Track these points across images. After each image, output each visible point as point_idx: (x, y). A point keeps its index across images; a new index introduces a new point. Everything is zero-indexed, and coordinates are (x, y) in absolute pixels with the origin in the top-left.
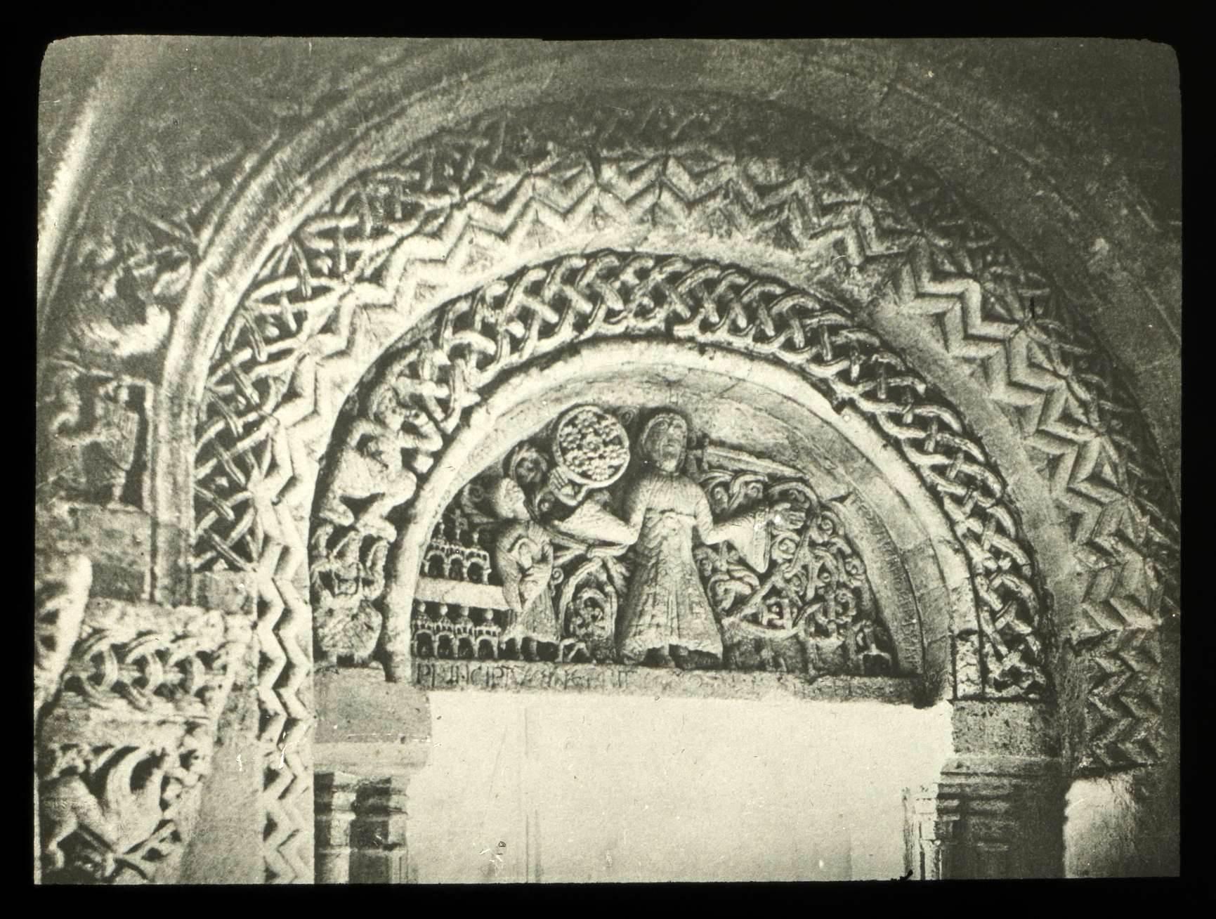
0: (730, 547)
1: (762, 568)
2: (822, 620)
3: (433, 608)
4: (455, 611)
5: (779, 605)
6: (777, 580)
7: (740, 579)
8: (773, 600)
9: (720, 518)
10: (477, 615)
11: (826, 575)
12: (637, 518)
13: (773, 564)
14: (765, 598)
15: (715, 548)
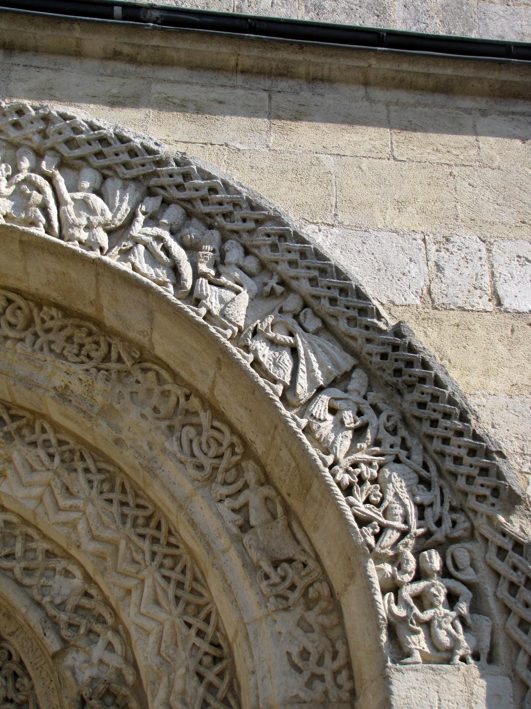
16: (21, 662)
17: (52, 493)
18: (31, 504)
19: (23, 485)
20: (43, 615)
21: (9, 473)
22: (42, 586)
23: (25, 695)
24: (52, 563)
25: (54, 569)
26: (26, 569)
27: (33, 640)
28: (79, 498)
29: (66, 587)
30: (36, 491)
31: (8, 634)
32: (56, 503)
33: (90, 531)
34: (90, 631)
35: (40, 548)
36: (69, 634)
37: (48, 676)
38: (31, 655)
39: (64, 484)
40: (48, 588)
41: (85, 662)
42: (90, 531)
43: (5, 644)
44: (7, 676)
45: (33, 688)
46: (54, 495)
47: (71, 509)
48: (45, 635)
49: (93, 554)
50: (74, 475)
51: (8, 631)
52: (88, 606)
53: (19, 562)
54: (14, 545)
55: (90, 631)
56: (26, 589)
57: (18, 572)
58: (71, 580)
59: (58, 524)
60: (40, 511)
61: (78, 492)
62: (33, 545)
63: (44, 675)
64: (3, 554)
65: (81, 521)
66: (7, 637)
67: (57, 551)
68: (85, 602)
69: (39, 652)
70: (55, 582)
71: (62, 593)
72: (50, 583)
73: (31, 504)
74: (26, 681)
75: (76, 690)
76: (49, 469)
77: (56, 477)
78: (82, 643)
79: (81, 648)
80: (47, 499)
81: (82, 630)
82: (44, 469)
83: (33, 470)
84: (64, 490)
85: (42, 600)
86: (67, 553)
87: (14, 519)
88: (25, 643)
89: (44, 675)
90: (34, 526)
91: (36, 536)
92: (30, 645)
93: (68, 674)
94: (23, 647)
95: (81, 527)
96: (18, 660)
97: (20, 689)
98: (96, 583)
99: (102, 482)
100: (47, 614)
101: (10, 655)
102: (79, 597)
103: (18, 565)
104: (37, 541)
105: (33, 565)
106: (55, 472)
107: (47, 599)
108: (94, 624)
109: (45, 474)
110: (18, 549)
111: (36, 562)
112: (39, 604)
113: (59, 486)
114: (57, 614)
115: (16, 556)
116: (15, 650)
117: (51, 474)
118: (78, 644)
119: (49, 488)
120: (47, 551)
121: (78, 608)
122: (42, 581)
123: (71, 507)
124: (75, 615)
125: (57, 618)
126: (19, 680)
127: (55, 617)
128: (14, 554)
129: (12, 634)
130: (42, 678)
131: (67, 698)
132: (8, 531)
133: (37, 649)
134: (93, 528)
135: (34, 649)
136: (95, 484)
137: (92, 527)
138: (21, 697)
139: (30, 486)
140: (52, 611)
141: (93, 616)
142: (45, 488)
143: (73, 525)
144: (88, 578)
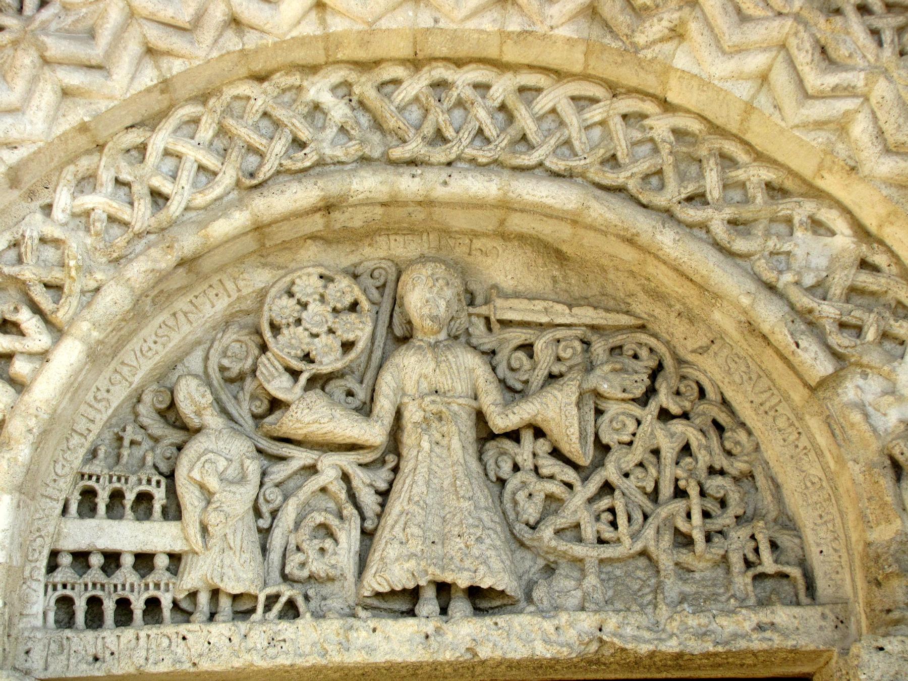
0: (539, 433)
1: (585, 456)
2: (683, 526)
3: (81, 558)
4: (112, 559)
5: (612, 510)
6: (611, 472)
7: (552, 477)
8: (605, 503)
9: (514, 392)
10: (144, 561)
11: (688, 460)
12: (384, 406)
13: (603, 449)
14: (591, 501)
15: (514, 436)
16: (725, 402)
17: (791, 63)
18: (743, 91)
19: (724, 53)
20: (787, 309)
21: (694, 27)
22: (771, 253)
23: (746, 462)
24: (784, 208)
25: (789, 221)
26: (733, 223)
27: (749, 361)
28: (853, 69)
29: (821, 253)
30: (755, 62)
31: (693, 351)
32: (800, 82)
33: (880, 133)
34: (885, 335)
35: (755, 180)
36: (846, 342)
37: (792, 424)
38: (749, 389)
39: (817, 41)
40: (782, 258)
41: (885, 393)
42: (880, 133)
43: (690, 370)
44: (705, 428)
45: (757, 448)
46: (795, 68)
47: (837, 92)
48: (798, 345)
49: (889, 183)
50: (838, 19)
51: (691, 344)
52: (874, 288)
53: (718, 209)
54: (701, 176)
55: (885, 335)
56: (739, 261)
57: (719, 229)
58: (828, 240)
59: (804, 126)
60: (763, 101)
61: (850, 56)
62: (740, 174)
63: (781, 423)
64: (683, 196)
65: (860, 116)
66: (690, 357)
67: (789, 184)
68: (865, 279)
69: (765, 383)
70: (796, 245)
71: (813, 265)
72: (786, 247)
73: (743, 91)
74: (742, 436)
75: (875, 445)
76: (780, 14)
77: (801, 28)
78: (873, 357)
79: (871, 368)
80: (781, 77)
81: (871, 334)
82: (770, 14)
83: (743, 18)
84: (817, 56)
85: (778, 280)
86: (811, 186)
87: (695, 126)
88: (733, 365)
89: (781, 423)
90: (735, 136)
91: (741, 156)
92: (744, 368)
93: (856, 417)
94: (729, 372)
95: (861, 129)
96: (719, 398)
97: (734, 451)
98: (881, 242)
99: (900, 30)
100: (792, 306)
101: (702, 393)
102: (853, 271)
103: (717, 215)
104: (746, 165)
105: (746, 213)
106: (797, 17)
107: (788, 277)
108: (892, 322)
109: (777, 23)
110: (712, 182)
111: (751, 207)
112: (771, 288)
113: (807, 46)
114: (815, 305)
115: (709, 198)
116: (711, 380)
117: (789, 23)
118: (865, 360)
119: (783, 53)
120: (768, 185)
121: (853, 291)
122: (770, 244)
123: (834, 89)
124: (850, 306)
125: (817, 314)
126: (728, 434)
127: (810, 311)
128: (703, 195)
129: (702, 351)
130: (780, 430)
131: (856, 461)
132: (684, 149)
133: (759, 377)
134: (889, 128)
135: (754, 377)
136: (887, 36)
137: (885, 127)
138: (738, 466)
139: (740, 51)
140: (805, 301)
141: (887, 306)
142: (774, 53)
143: (841, 126)
144: (862, 232)
